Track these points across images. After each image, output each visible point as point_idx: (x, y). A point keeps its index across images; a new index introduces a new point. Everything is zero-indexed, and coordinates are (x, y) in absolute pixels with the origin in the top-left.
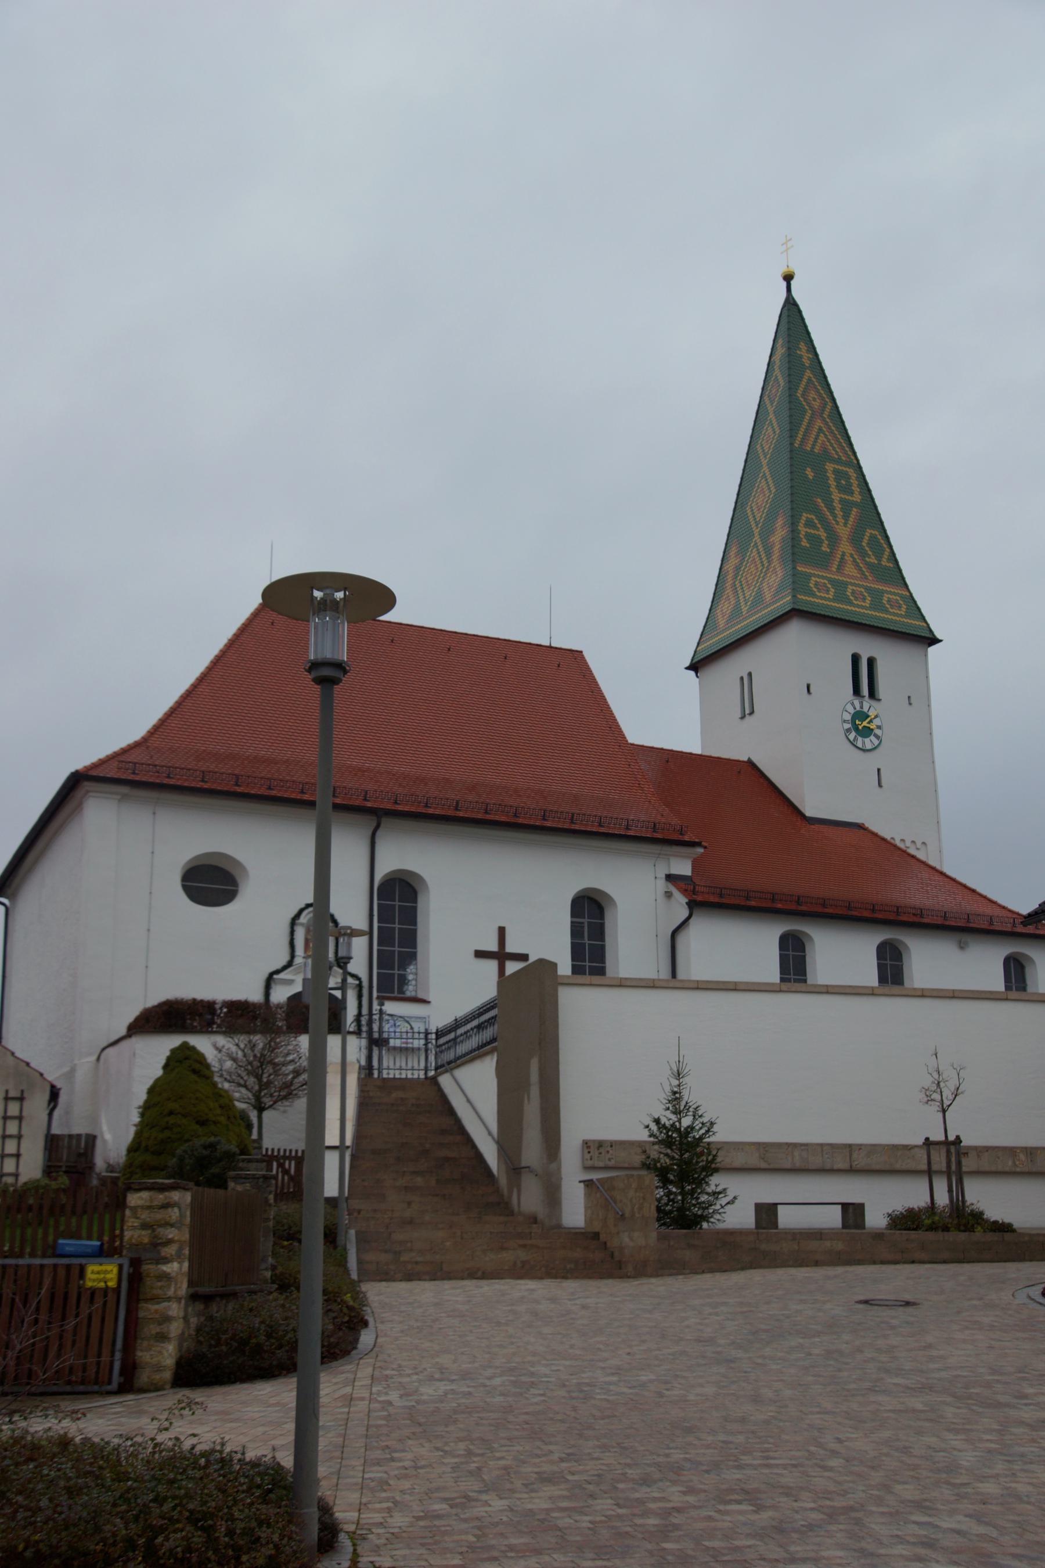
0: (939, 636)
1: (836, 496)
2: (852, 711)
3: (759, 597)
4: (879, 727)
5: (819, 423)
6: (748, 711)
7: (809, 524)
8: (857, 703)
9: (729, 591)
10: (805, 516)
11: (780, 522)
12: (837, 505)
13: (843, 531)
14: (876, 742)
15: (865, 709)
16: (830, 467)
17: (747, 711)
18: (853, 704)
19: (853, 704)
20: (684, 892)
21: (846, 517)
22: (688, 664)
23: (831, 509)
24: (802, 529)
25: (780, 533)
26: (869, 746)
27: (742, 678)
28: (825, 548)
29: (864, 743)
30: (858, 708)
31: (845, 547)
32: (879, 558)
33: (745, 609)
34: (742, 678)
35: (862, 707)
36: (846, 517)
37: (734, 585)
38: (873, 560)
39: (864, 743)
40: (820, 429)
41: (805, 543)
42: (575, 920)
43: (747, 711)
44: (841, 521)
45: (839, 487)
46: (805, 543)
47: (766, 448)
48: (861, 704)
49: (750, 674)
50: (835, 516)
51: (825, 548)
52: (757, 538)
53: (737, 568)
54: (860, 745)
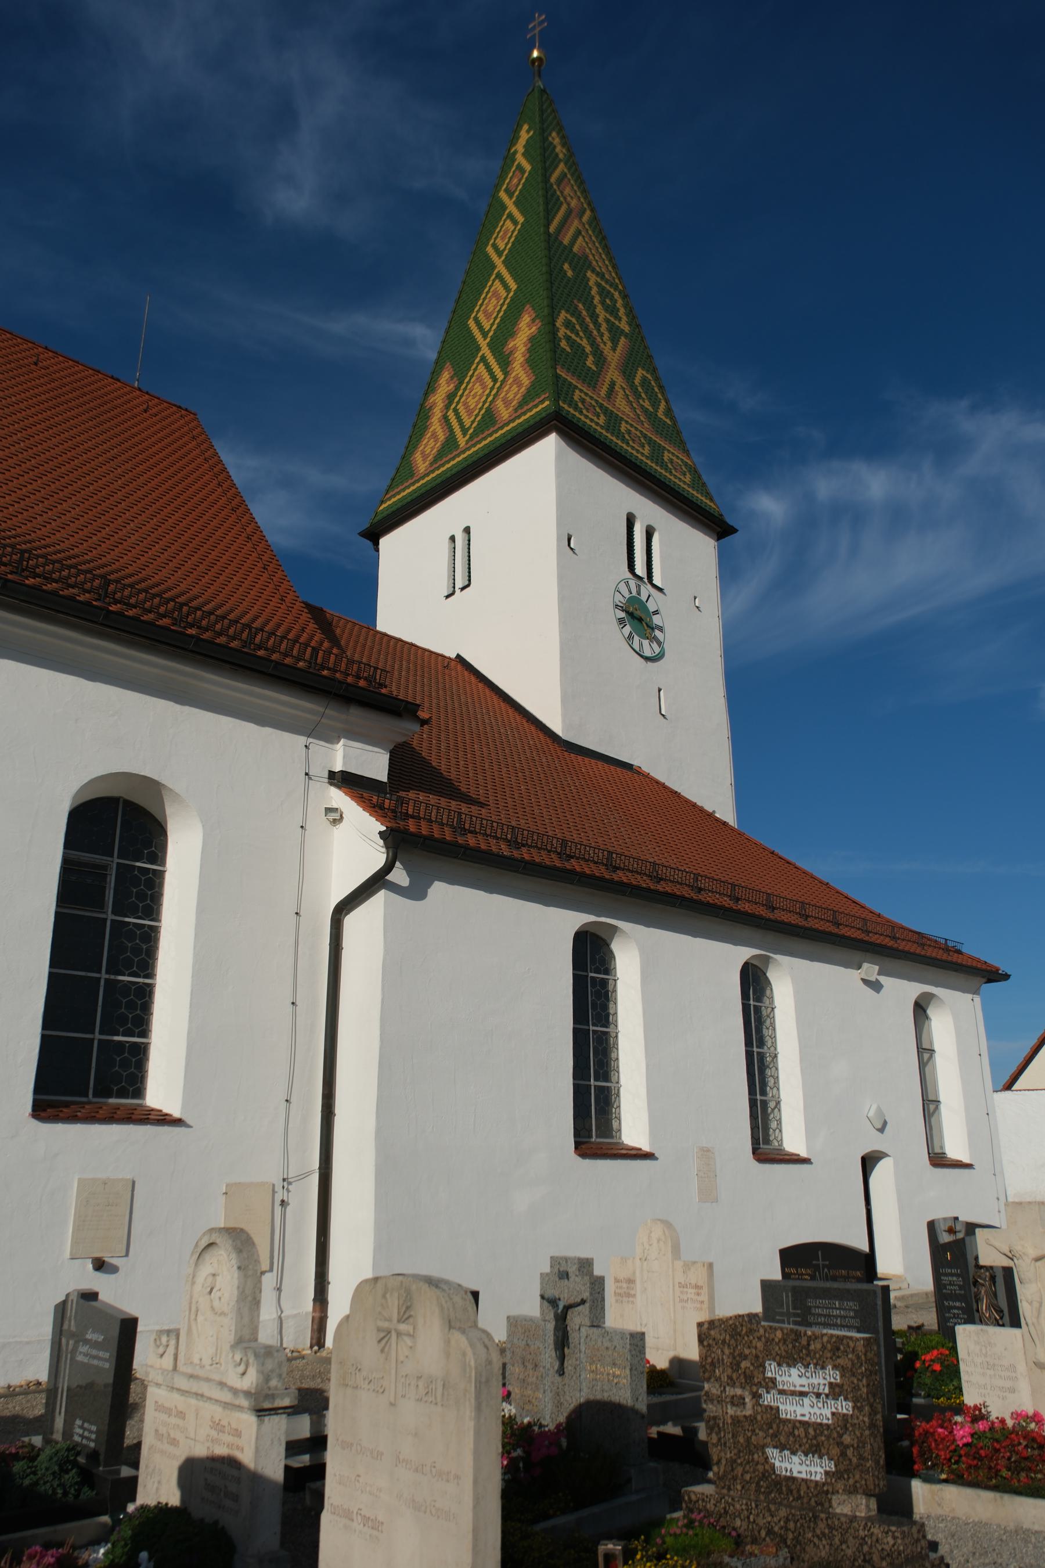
0: (730, 520)
1: (602, 314)
2: (627, 595)
3: (489, 418)
4: (661, 629)
5: (576, 223)
6: (461, 580)
7: (568, 324)
8: (633, 584)
9: (436, 424)
10: (563, 314)
11: (526, 319)
12: (604, 326)
13: (614, 357)
14: (657, 650)
15: (644, 598)
16: (592, 278)
17: (459, 584)
18: (627, 584)
19: (627, 584)
20: (375, 809)
21: (615, 343)
22: (366, 525)
23: (598, 326)
24: (562, 332)
25: (526, 328)
26: (648, 653)
27: (453, 539)
28: (590, 362)
29: (641, 645)
30: (634, 593)
31: (613, 374)
32: (655, 404)
33: (462, 441)
34: (453, 539)
35: (639, 593)
36: (615, 343)
37: (445, 418)
38: (647, 404)
39: (641, 645)
40: (578, 233)
41: (563, 344)
42: (75, 854)
43: (459, 584)
44: (609, 344)
45: (603, 303)
46: (563, 344)
47: (502, 246)
48: (638, 587)
49: (467, 530)
50: (602, 335)
51: (590, 362)
52: (485, 350)
53: (450, 397)
54: (636, 646)
